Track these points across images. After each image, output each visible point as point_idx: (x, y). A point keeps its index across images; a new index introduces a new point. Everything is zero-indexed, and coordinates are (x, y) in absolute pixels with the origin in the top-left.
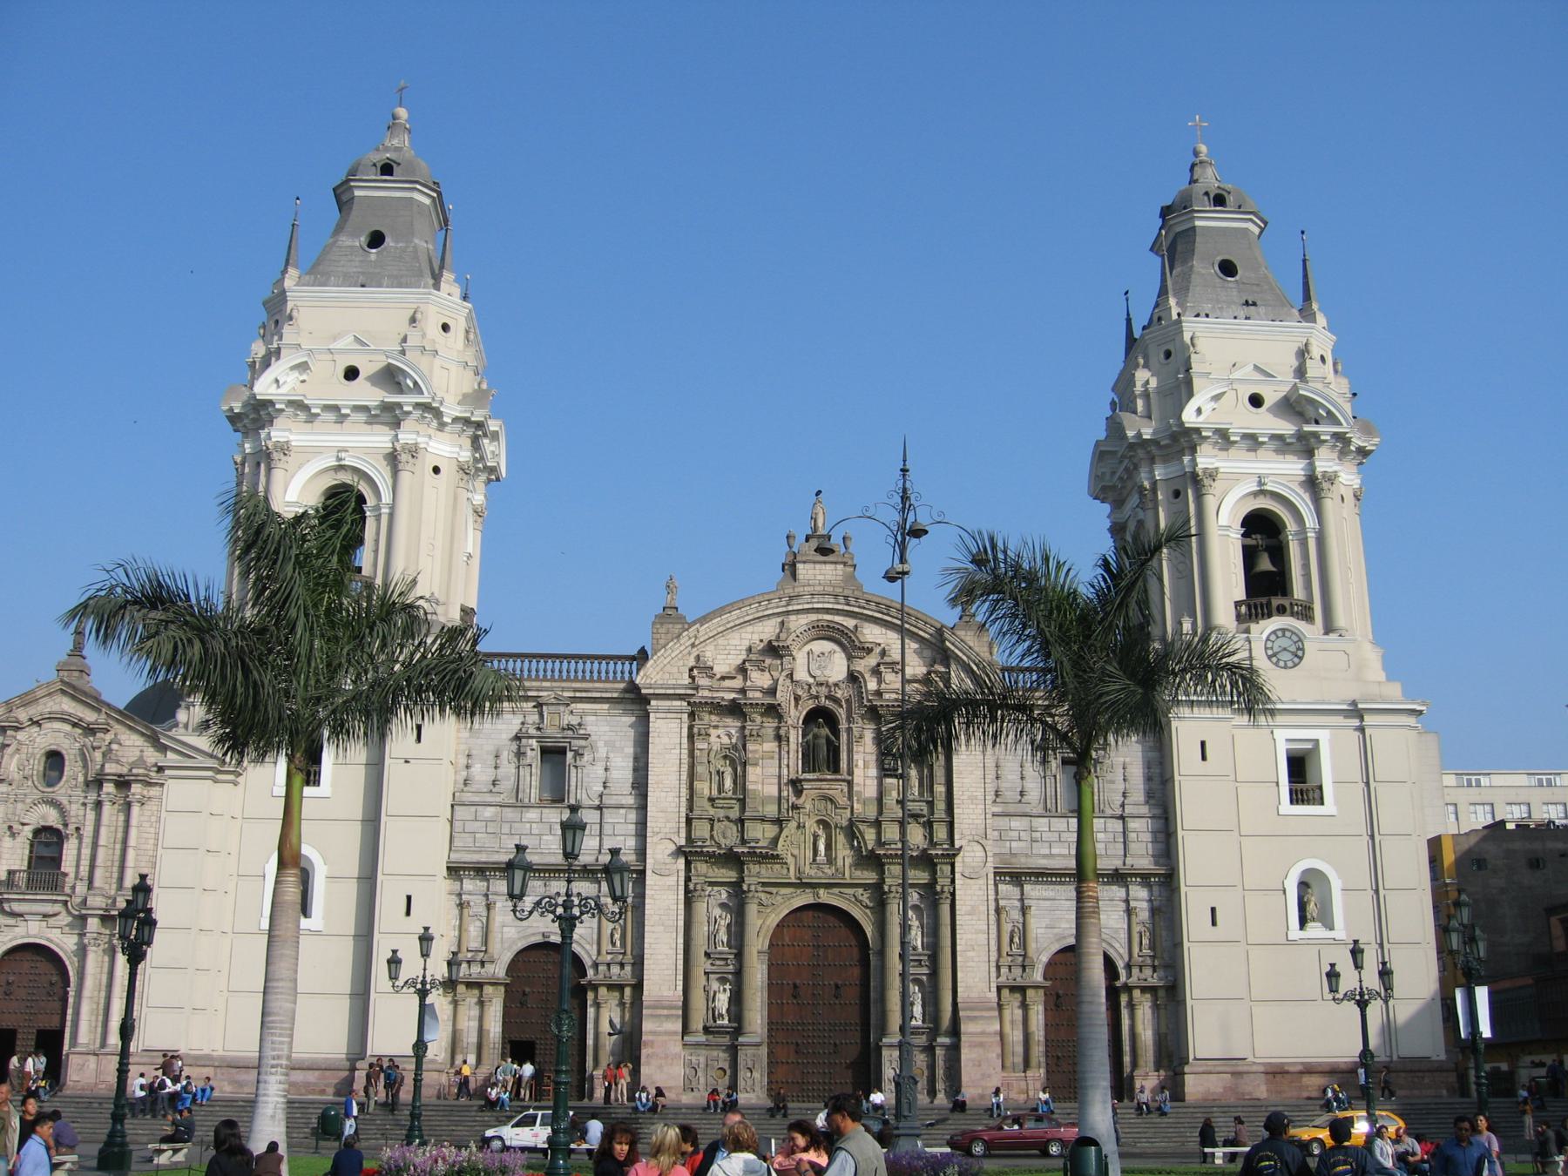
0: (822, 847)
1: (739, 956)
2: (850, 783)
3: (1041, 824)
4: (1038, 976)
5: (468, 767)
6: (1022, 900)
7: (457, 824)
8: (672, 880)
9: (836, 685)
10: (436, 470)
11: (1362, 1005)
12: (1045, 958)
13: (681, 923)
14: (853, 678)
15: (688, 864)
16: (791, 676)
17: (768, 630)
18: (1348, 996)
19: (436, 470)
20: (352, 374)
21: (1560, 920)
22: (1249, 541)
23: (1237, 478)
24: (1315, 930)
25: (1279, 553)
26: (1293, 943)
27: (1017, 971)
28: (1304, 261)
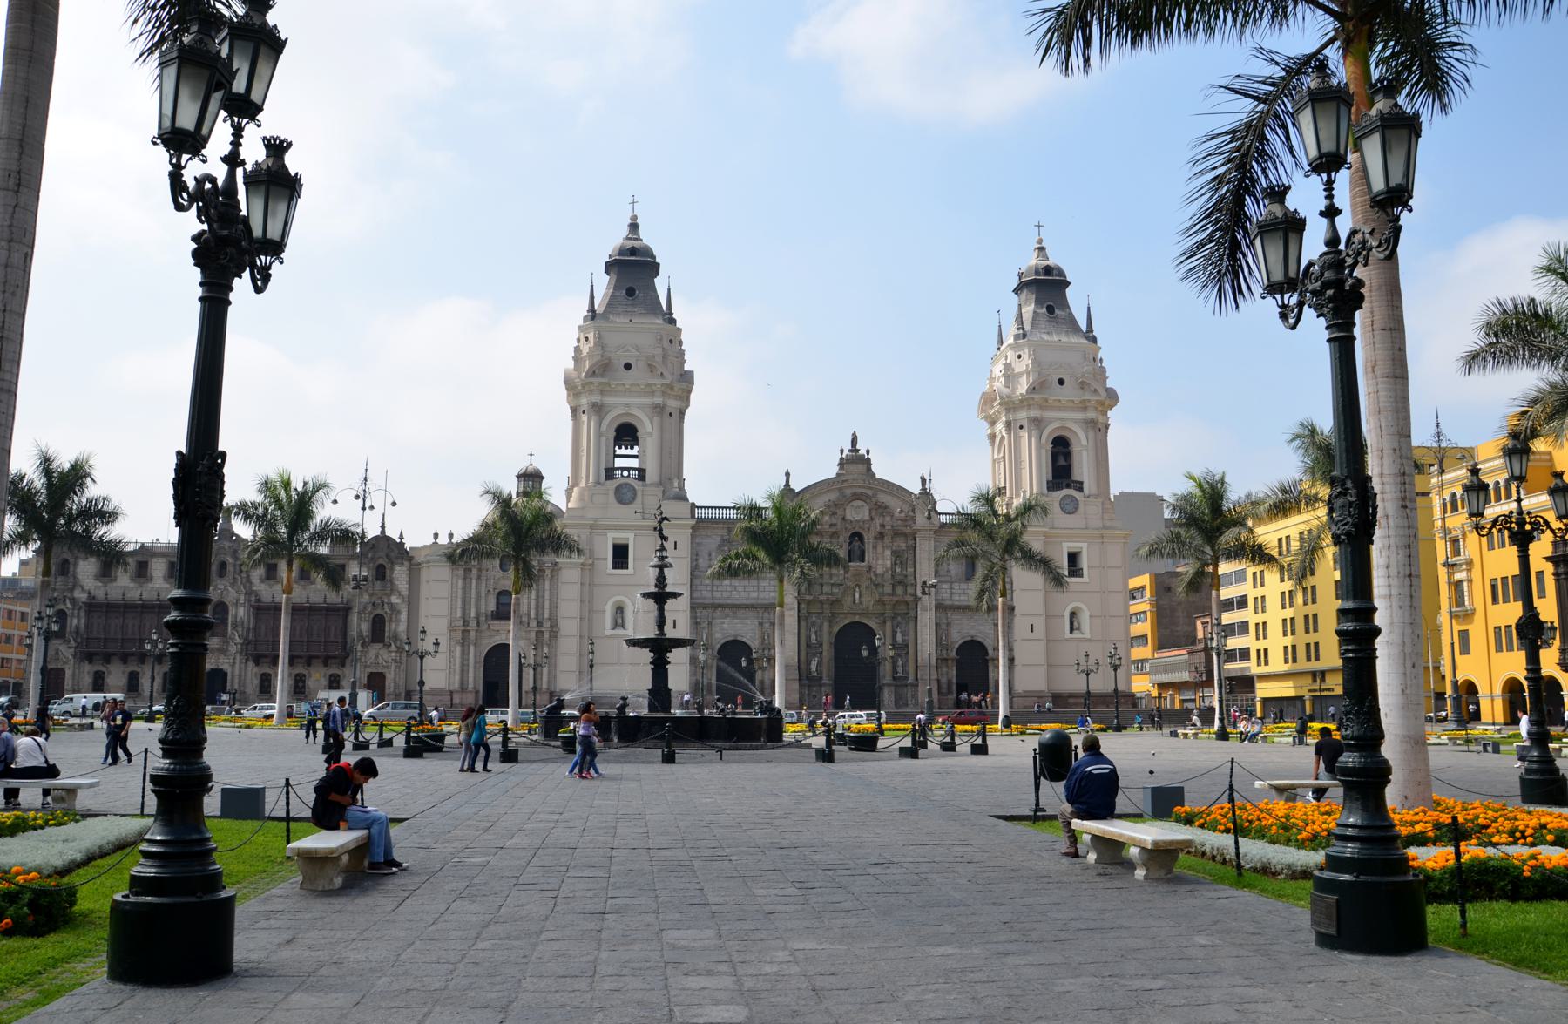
0: (857, 596)
1: (821, 645)
2: (870, 567)
3: (956, 586)
4: (953, 654)
5: (697, 560)
6: (947, 619)
7: (694, 587)
8: (792, 612)
9: (864, 522)
10: (671, 414)
11: (1088, 674)
12: (957, 646)
13: (796, 631)
14: (872, 519)
15: (799, 604)
16: (843, 519)
17: (833, 496)
18: (1083, 671)
19: (671, 414)
20: (628, 366)
21: (1203, 623)
22: (1056, 450)
23: (1051, 421)
24: (1076, 635)
25: (1068, 455)
26: (1067, 640)
27: (944, 652)
28: (1089, 308)
